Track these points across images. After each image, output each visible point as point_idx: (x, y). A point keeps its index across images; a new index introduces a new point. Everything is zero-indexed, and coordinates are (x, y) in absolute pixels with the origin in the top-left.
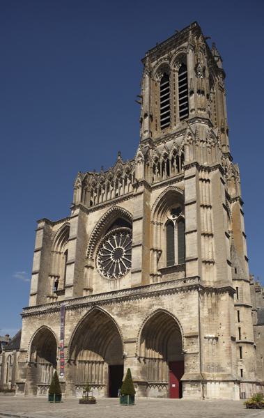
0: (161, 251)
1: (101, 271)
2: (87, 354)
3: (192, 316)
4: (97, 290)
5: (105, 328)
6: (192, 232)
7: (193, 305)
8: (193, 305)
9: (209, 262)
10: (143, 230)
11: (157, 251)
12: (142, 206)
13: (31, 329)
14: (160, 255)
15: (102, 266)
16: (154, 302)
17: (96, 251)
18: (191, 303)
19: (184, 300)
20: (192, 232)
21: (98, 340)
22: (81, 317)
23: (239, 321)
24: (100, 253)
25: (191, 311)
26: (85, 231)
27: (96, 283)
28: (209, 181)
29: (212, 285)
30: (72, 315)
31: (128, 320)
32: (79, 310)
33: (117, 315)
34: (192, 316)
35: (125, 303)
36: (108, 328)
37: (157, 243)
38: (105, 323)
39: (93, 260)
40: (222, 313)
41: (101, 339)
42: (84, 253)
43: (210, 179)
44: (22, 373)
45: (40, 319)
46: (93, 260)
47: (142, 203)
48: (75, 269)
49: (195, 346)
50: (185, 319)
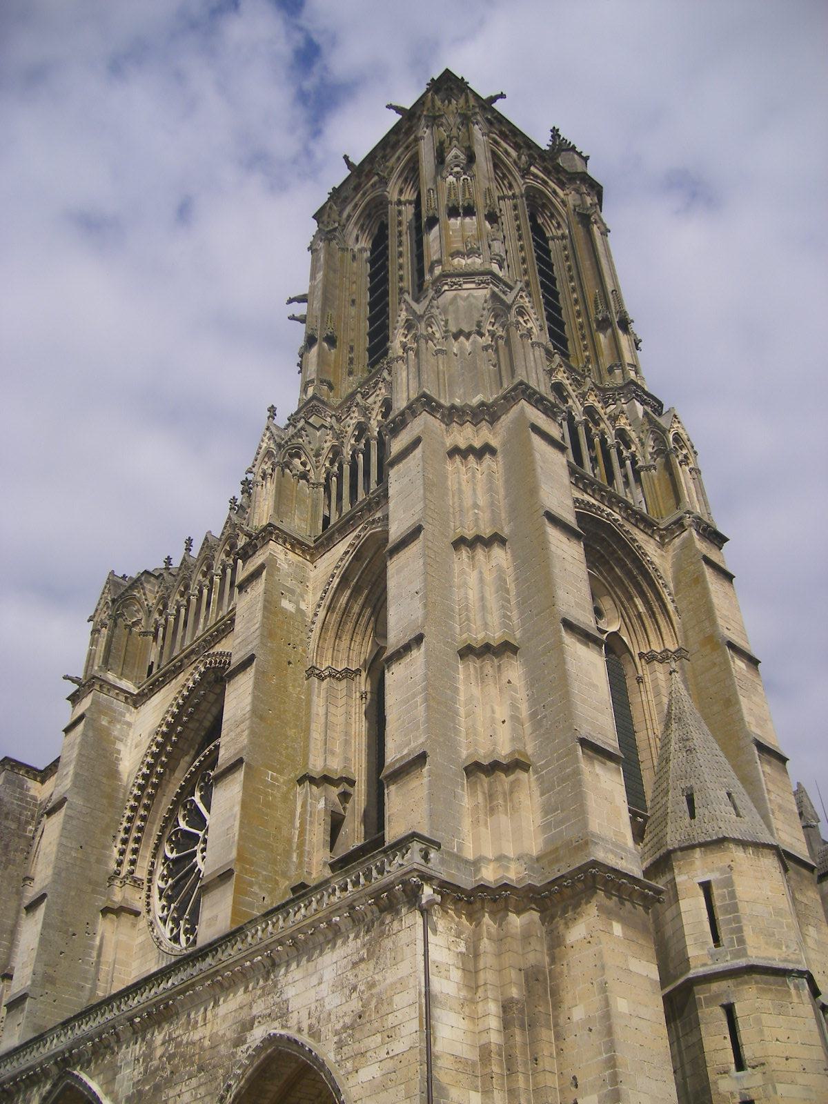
0: (352, 783)
1: (164, 921)
3: (399, 1047)
9: (494, 767)
10: (255, 698)
11: (326, 780)
12: (259, 616)
14: (345, 797)
15: (170, 899)
19: (366, 971)
23: (740, 1065)
24: (167, 848)
26: (114, 773)
28: (493, 451)
29: (514, 874)
34: (399, 1047)
37: (328, 751)
39: (137, 883)
40: (578, 1014)
42: (102, 860)
43: (494, 443)
46: (137, 883)
47: (260, 605)
48: (46, 925)
50: (370, 1072)
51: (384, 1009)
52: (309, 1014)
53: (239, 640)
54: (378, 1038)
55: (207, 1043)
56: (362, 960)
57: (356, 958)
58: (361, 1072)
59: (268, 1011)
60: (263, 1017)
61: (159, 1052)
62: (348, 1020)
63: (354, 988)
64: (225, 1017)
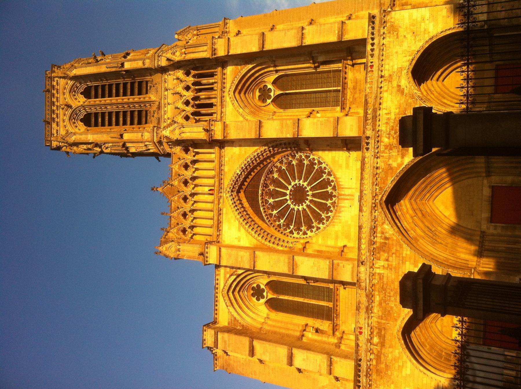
4: (348, 237)
6: (303, 34)
13: (400, 368)
16: (395, 84)
17: (282, 237)
19: (402, 32)
20: (303, 34)
25: (419, 19)
27: (337, 238)
30: (387, 260)
32: (379, 240)
33: (403, 157)
35: (386, 140)
38: (411, 212)
41: (439, 228)
45: (382, 344)
52: (405, 57)
53: (247, 134)
54: (423, 24)
55: (397, 111)
56: (397, 34)
57: (396, 37)
58: (430, 31)
59: (398, 78)
60: (399, 79)
61: (392, 140)
62: (413, 38)
63: (405, 36)
64: (392, 101)
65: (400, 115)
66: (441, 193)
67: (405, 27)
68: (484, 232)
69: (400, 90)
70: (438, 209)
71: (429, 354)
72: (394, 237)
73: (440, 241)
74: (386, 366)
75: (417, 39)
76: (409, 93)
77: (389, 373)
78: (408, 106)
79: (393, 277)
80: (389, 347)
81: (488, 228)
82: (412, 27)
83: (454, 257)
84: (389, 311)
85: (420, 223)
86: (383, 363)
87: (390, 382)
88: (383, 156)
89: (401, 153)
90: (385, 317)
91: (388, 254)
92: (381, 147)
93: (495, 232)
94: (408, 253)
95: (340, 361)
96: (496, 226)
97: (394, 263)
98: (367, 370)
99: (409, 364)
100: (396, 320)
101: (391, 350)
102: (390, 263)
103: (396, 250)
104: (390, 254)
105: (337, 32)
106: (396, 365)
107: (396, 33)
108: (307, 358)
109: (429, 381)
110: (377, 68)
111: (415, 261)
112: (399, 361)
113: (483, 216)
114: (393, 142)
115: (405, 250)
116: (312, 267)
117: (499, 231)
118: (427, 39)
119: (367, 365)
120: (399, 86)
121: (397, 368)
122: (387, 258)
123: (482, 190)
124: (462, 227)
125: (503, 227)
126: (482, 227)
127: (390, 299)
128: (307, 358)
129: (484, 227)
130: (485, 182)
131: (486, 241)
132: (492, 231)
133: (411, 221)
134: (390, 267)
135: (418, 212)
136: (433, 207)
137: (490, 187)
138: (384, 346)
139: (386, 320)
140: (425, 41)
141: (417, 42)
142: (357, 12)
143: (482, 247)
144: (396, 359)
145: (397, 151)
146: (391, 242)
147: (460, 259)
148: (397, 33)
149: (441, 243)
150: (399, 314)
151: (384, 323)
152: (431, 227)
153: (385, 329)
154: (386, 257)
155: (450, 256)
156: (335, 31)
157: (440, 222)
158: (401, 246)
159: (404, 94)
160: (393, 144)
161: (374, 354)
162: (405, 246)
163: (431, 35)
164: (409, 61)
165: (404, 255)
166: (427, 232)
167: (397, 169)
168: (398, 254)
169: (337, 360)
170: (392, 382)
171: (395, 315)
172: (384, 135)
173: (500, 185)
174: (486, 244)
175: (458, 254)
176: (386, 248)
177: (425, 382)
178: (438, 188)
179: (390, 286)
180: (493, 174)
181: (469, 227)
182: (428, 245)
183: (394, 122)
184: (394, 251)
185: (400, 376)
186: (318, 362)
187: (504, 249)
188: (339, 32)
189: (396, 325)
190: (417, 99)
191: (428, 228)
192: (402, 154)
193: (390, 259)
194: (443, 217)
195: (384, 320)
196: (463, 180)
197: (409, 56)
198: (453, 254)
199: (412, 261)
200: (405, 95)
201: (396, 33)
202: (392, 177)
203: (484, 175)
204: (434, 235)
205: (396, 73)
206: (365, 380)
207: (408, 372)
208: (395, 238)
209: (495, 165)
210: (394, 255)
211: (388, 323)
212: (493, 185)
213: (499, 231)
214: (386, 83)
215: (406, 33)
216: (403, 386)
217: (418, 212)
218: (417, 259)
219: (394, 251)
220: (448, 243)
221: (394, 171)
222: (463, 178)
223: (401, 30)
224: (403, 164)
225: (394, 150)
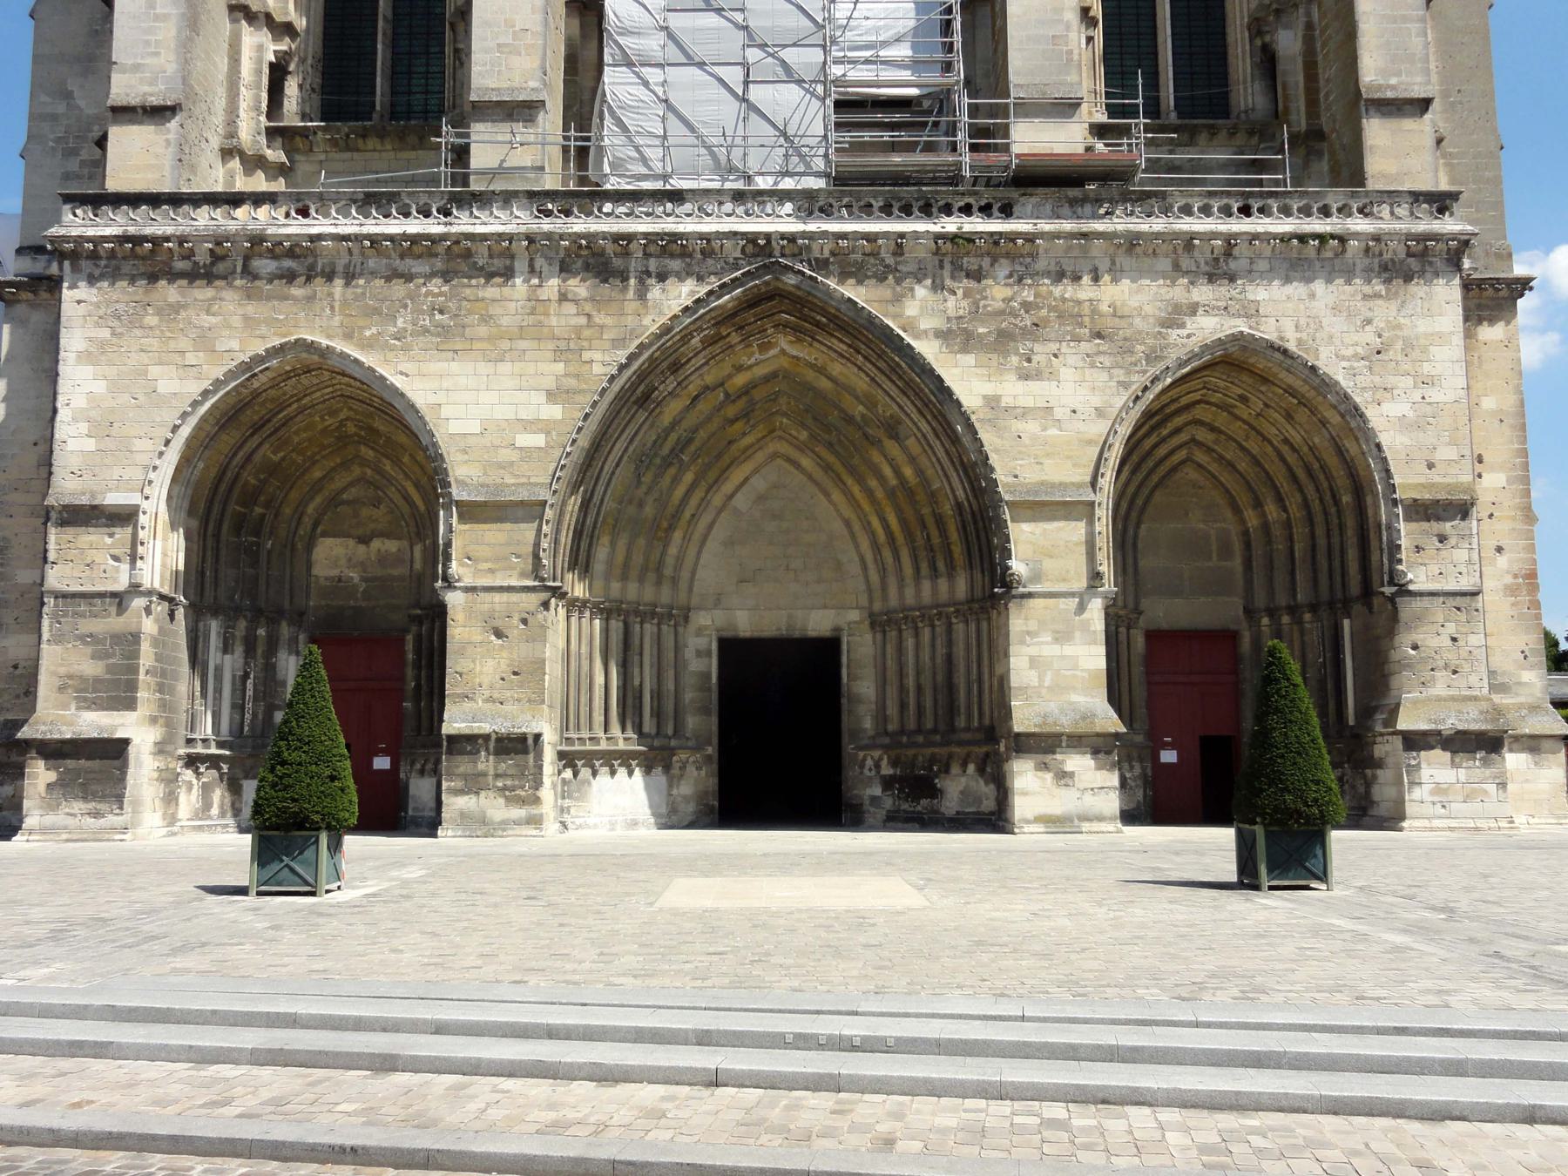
2: (610, 563)
3: (1435, 395)
5: (731, 411)
7: (1441, 338)
8: (1441, 338)
18: (1423, 326)
19: (1384, 311)
21: (676, 480)
22: (651, 324)
31: (1025, 376)
36: (745, 415)
38: (740, 380)
41: (689, 477)
44: (91, 668)
49: (1461, 555)
51: (1415, 354)
52: (1296, 327)
55: (1104, 308)
60: (1218, 308)
63: (1369, 322)
65: (1092, 319)
66: (810, 477)
67: (1402, 321)
68: (686, 619)
69: (1175, 316)
70: (756, 471)
71: (248, 458)
72: (650, 318)
73: (647, 479)
74: (176, 308)
75: (1356, 364)
76: (1169, 344)
77: (151, 320)
78: (1121, 344)
79: (505, 321)
80: (246, 318)
81: (699, 632)
82: (1399, 345)
83: (594, 527)
84: (376, 311)
85: (703, 407)
86: (183, 297)
87: (116, 323)
88: (942, 267)
89: (954, 327)
90: (355, 299)
91: (585, 300)
92: (973, 260)
93: (689, 653)
94: (597, 369)
95: (168, 142)
96: (709, 653)
97: (554, 321)
98: (145, 239)
99: (195, 388)
100: (348, 336)
101: (236, 321)
102: (553, 307)
103: (602, 327)
104: (588, 308)
105: (1393, 81)
106: (184, 343)
107: (1383, 293)
108: (157, 18)
109: (143, 459)
110: (1260, 229)
111: (567, 392)
112: (201, 354)
113: (739, 613)
114: (993, 299)
115: (607, 358)
116: (510, 24)
117: (695, 665)
118: (1358, 399)
119: (167, 239)
120: (1193, 309)
121: (172, 345)
122: (570, 296)
123: (825, 607)
124: (699, 553)
125: (708, 676)
126: (702, 613)
127: (422, 312)
128: (157, 18)
129: (702, 619)
130: (854, 615)
131: (659, 624)
132: (694, 643)
133: (709, 379)
134: (540, 309)
135: (741, 404)
136: (760, 457)
137: (838, 629)
138: (249, 297)
139: (345, 302)
140: (1349, 391)
141: (1345, 364)
142: (1446, 165)
143: (637, 613)
144: (204, 341)
145: (961, 312)
146: (632, 306)
147: (590, 545)
148: (1381, 296)
149: (639, 482)
150: (371, 346)
151: (330, 295)
152: (693, 448)
153: (311, 299)
154: (575, 294)
155: (598, 514)
156: (1398, 74)
157: (710, 481)
158: (618, 343)
159: (1164, 330)
160: (985, 298)
161: (213, 264)
162: (622, 356)
163: (1371, 413)
164: (1282, 339)
165: (586, 356)
166: (673, 437)
167: (895, 317)
168: (587, 333)
169: (169, 131)
170: (119, 330)
171: (368, 333)
172: (1018, 267)
173: (844, 659)
174: (647, 626)
175: (605, 540)
176: (607, 292)
177: (138, 445)
178: (827, 468)
179: (470, 312)
180: (879, 636)
181: (700, 573)
182: (631, 441)
183: (1064, 300)
184: (599, 319)
185: (145, 358)
186: (148, 61)
187: (637, 682)
188: (1393, 88)
189: (329, 337)
190: (1144, 372)
191: (690, 441)
192: (950, 331)
193: (570, 308)
194: (728, 487)
195: (343, 295)
196: (857, 546)
197: (1300, 342)
198: (603, 522)
199: (572, 382)
200: (1160, 333)
201: (1383, 293)
202: (866, 301)
203: (877, 606)
204: (663, 459)
205: (1242, 296)
206: (108, 232)
207: (164, 387)
208: (647, 321)
209: (910, 643)
210: (583, 320)
211: (332, 308)
212: (845, 640)
213: (695, 665)
214: (1207, 263)
215: (1382, 325)
216: (112, 371)
217: (741, 404)
218: (579, 398)
219: (599, 319)
220: (641, 505)
221: (891, 309)
222: (865, 545)
223: (1393, 306)
224: (917, 337)
225: (964, 303)
